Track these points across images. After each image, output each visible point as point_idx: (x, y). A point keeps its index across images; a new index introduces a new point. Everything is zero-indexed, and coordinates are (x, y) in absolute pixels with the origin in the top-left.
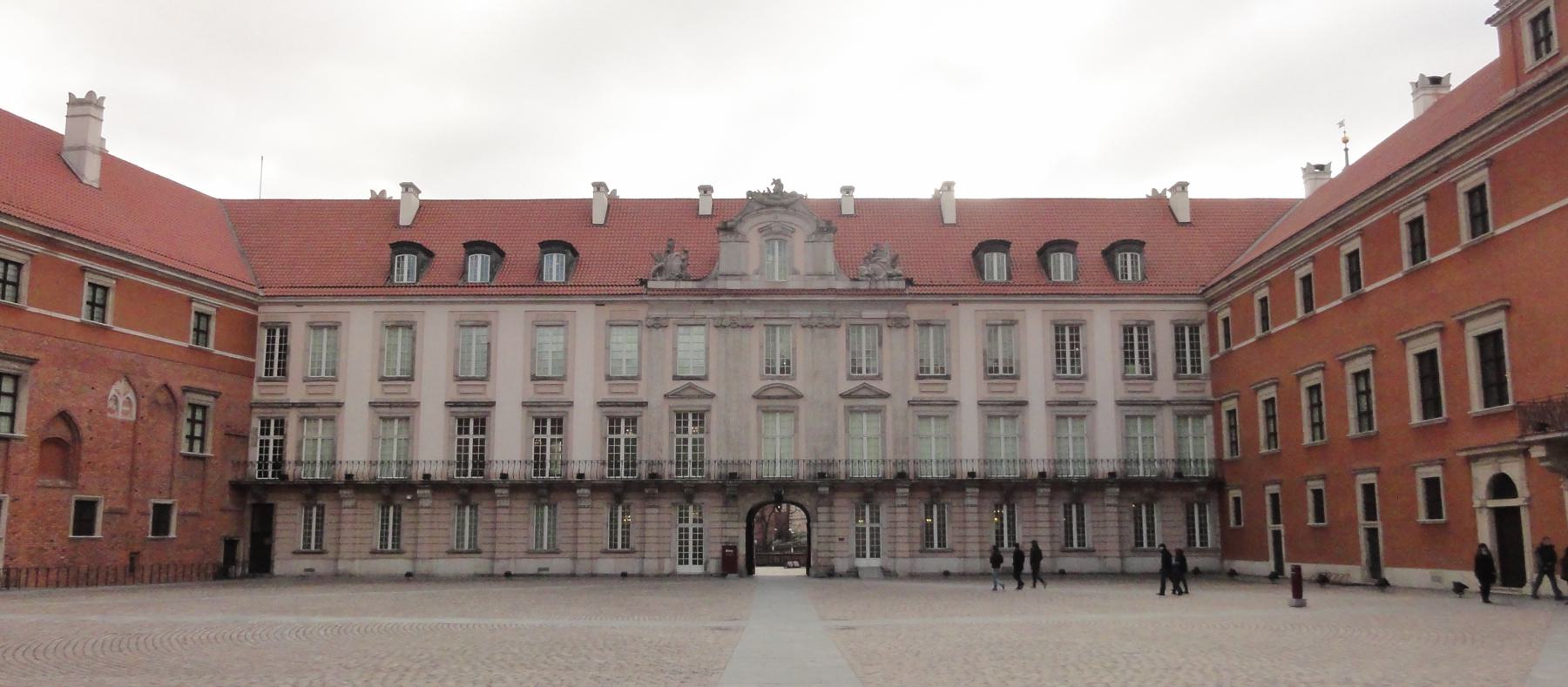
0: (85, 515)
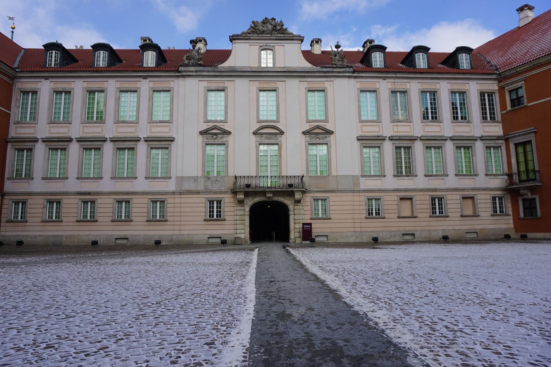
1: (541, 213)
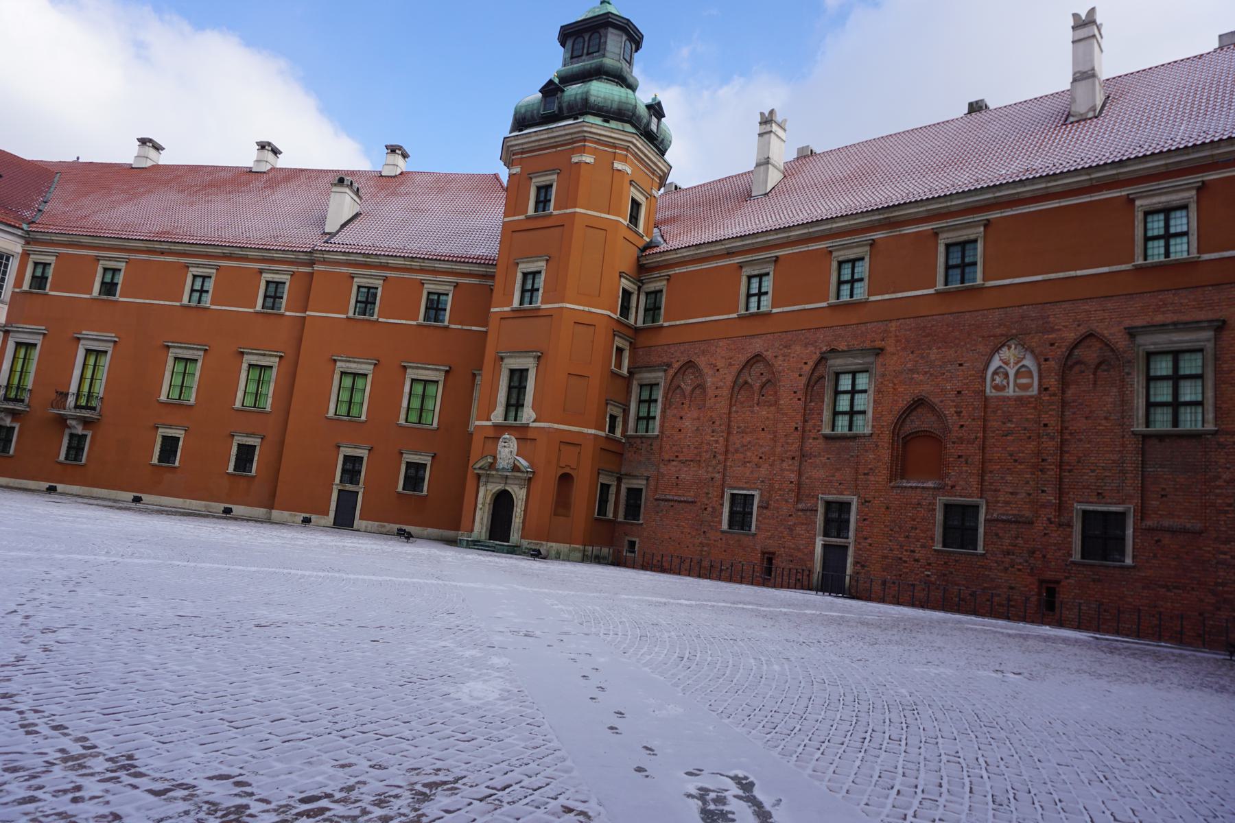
0: (959, 525)
1: (15, 450)
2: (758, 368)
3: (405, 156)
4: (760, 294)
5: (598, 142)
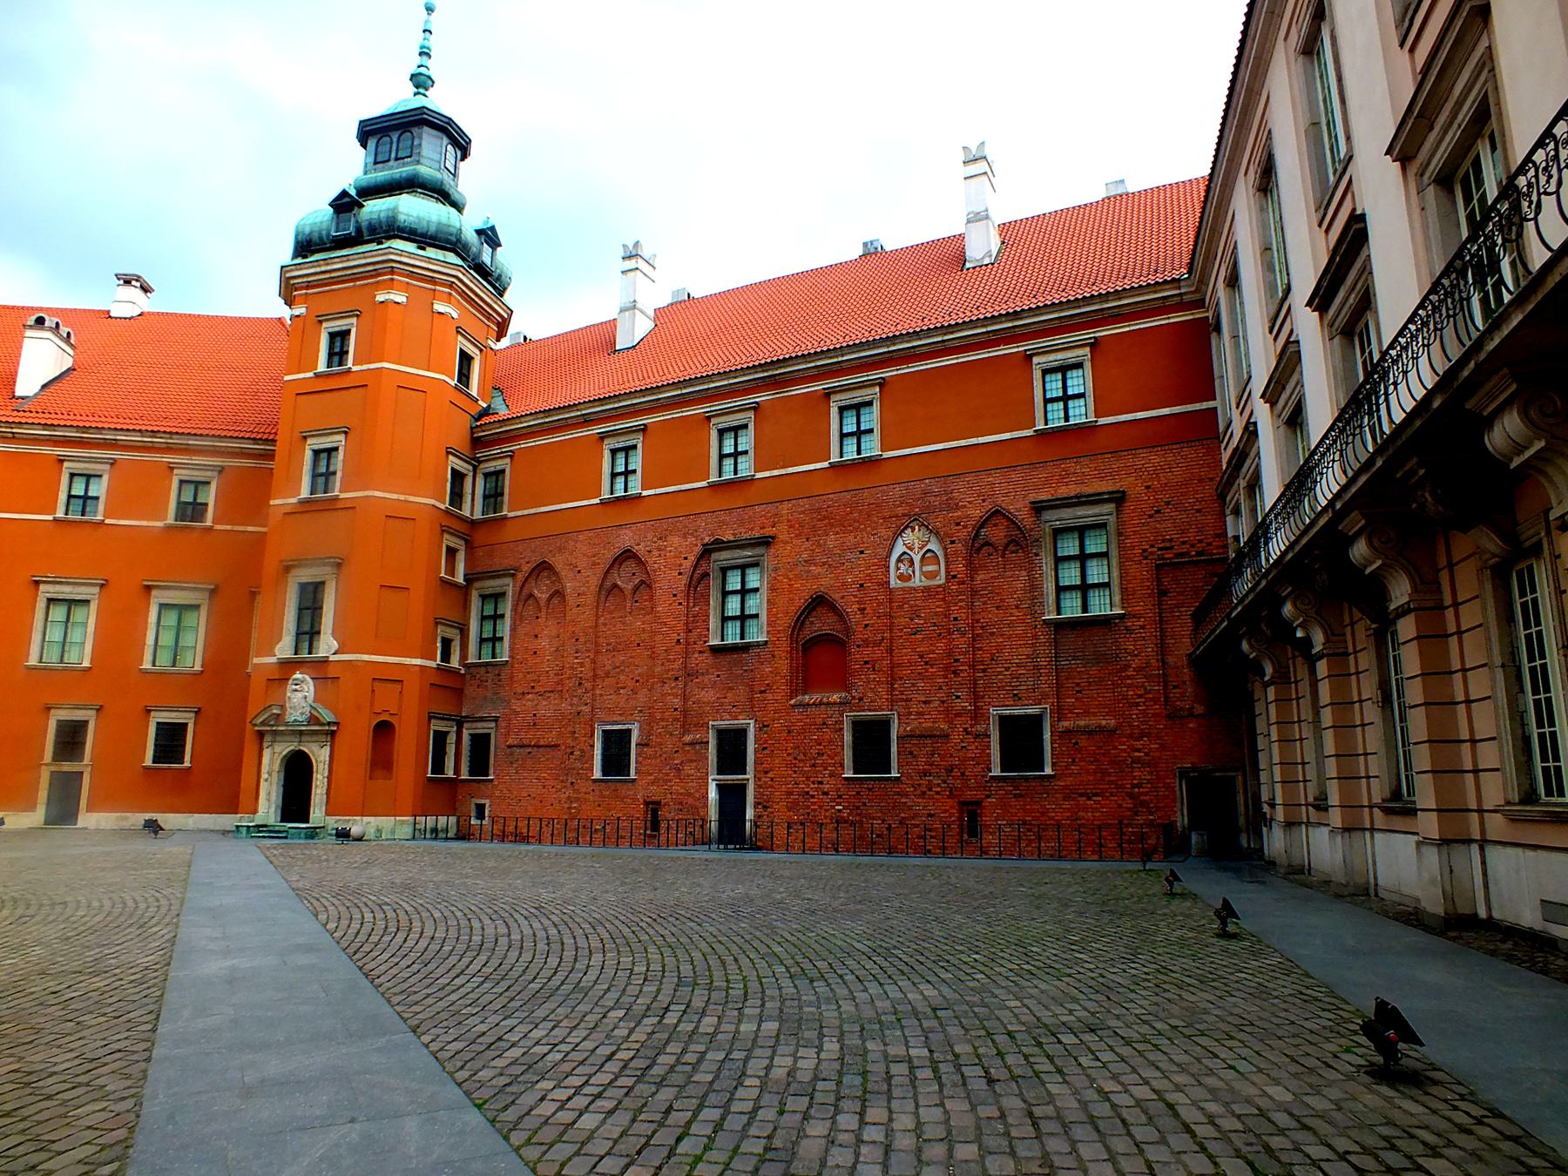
0: (871, 743)
2: (630, 566)
3: (146, 289)
4: (628, 473)
5: (411, 275)
